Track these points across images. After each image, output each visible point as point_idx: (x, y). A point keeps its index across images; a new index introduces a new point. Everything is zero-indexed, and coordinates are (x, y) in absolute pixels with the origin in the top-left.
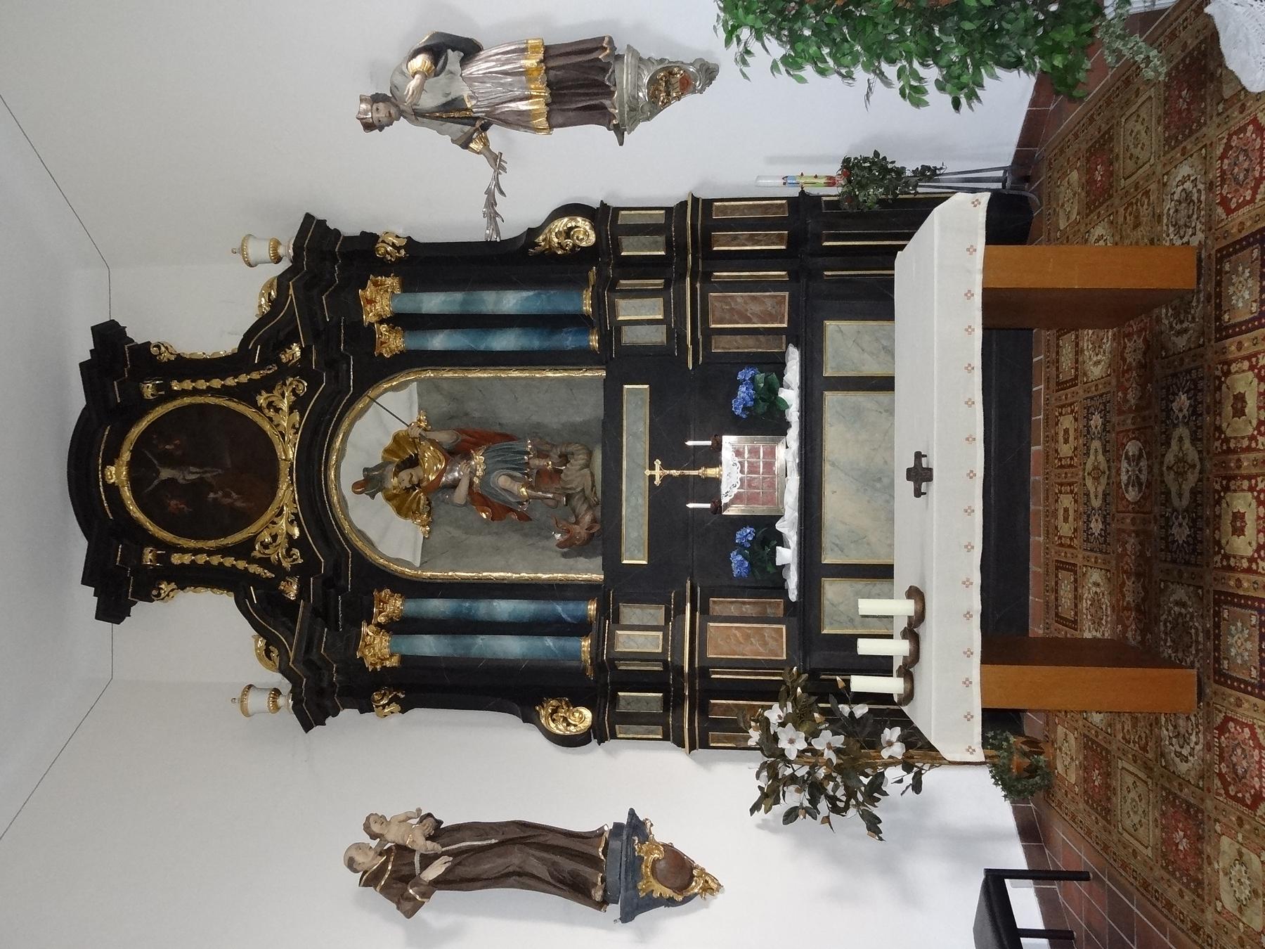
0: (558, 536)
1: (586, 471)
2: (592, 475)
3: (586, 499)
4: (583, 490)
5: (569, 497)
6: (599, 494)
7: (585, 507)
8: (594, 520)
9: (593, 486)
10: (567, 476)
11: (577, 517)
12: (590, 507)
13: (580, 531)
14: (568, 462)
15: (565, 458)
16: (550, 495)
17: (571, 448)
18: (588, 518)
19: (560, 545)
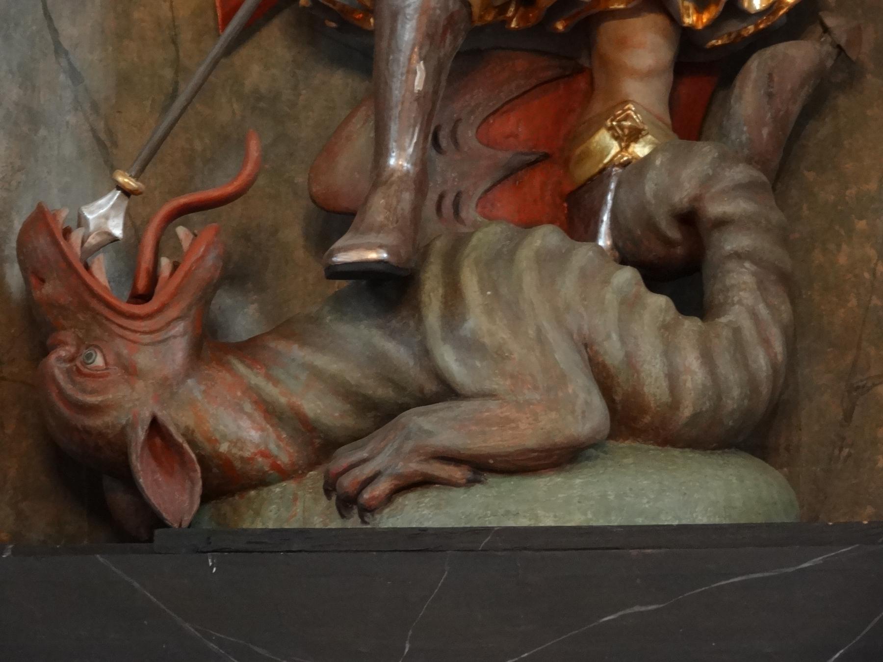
0: (105, 216)
1: (586, 414)
2: (563, 457)
3: (379, 413)
4: (447, 391)
5: (388, 290)
6: (419, 513)
7: (317, 406)
8: (226, 481)
9: (481, 467)
10: (550, 264)
11: (249, 350)
12: (320, 446)
13: (139, 379)
14: (656, 277)
15: (677, 265)
16: (399, 161)
17: (745, 299)
18: (242, 432)
19: (45, 239)
